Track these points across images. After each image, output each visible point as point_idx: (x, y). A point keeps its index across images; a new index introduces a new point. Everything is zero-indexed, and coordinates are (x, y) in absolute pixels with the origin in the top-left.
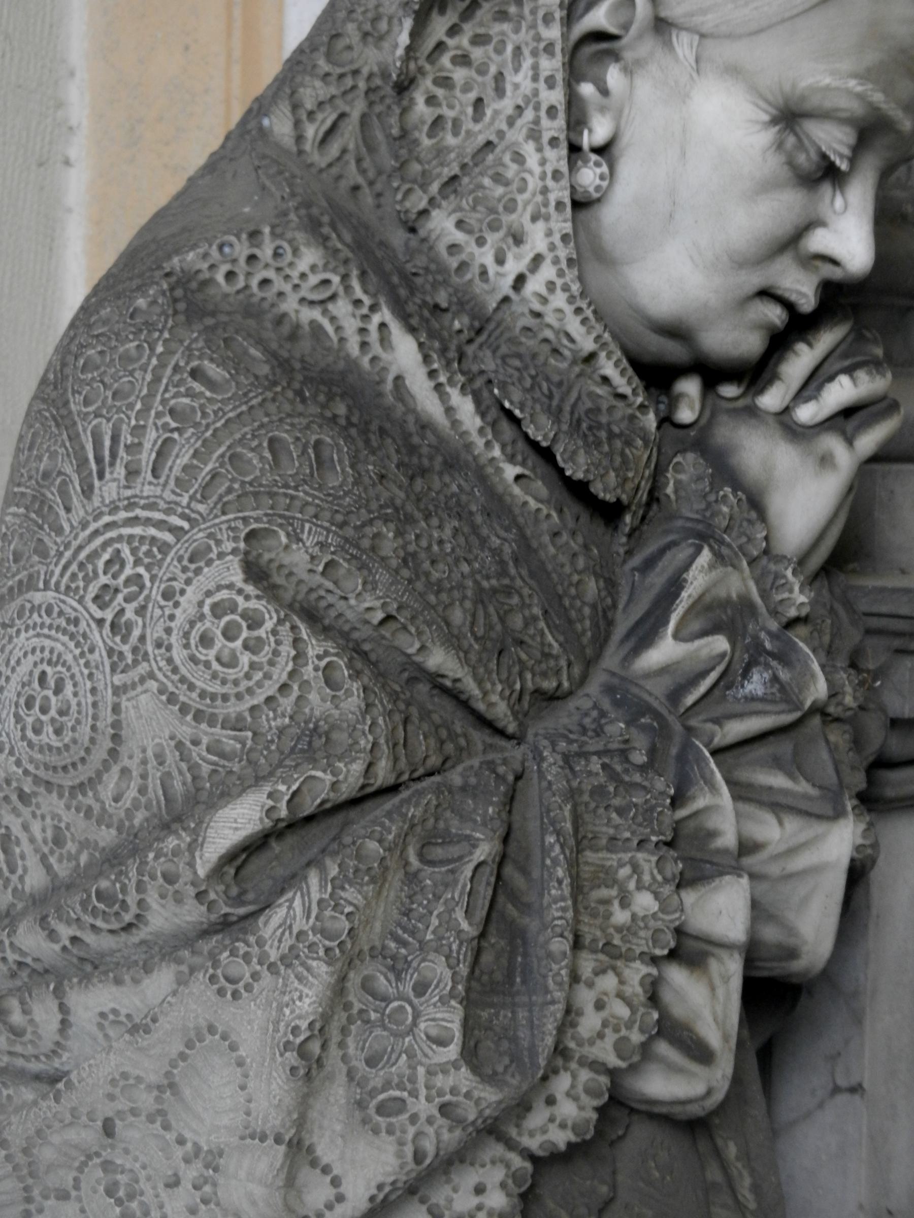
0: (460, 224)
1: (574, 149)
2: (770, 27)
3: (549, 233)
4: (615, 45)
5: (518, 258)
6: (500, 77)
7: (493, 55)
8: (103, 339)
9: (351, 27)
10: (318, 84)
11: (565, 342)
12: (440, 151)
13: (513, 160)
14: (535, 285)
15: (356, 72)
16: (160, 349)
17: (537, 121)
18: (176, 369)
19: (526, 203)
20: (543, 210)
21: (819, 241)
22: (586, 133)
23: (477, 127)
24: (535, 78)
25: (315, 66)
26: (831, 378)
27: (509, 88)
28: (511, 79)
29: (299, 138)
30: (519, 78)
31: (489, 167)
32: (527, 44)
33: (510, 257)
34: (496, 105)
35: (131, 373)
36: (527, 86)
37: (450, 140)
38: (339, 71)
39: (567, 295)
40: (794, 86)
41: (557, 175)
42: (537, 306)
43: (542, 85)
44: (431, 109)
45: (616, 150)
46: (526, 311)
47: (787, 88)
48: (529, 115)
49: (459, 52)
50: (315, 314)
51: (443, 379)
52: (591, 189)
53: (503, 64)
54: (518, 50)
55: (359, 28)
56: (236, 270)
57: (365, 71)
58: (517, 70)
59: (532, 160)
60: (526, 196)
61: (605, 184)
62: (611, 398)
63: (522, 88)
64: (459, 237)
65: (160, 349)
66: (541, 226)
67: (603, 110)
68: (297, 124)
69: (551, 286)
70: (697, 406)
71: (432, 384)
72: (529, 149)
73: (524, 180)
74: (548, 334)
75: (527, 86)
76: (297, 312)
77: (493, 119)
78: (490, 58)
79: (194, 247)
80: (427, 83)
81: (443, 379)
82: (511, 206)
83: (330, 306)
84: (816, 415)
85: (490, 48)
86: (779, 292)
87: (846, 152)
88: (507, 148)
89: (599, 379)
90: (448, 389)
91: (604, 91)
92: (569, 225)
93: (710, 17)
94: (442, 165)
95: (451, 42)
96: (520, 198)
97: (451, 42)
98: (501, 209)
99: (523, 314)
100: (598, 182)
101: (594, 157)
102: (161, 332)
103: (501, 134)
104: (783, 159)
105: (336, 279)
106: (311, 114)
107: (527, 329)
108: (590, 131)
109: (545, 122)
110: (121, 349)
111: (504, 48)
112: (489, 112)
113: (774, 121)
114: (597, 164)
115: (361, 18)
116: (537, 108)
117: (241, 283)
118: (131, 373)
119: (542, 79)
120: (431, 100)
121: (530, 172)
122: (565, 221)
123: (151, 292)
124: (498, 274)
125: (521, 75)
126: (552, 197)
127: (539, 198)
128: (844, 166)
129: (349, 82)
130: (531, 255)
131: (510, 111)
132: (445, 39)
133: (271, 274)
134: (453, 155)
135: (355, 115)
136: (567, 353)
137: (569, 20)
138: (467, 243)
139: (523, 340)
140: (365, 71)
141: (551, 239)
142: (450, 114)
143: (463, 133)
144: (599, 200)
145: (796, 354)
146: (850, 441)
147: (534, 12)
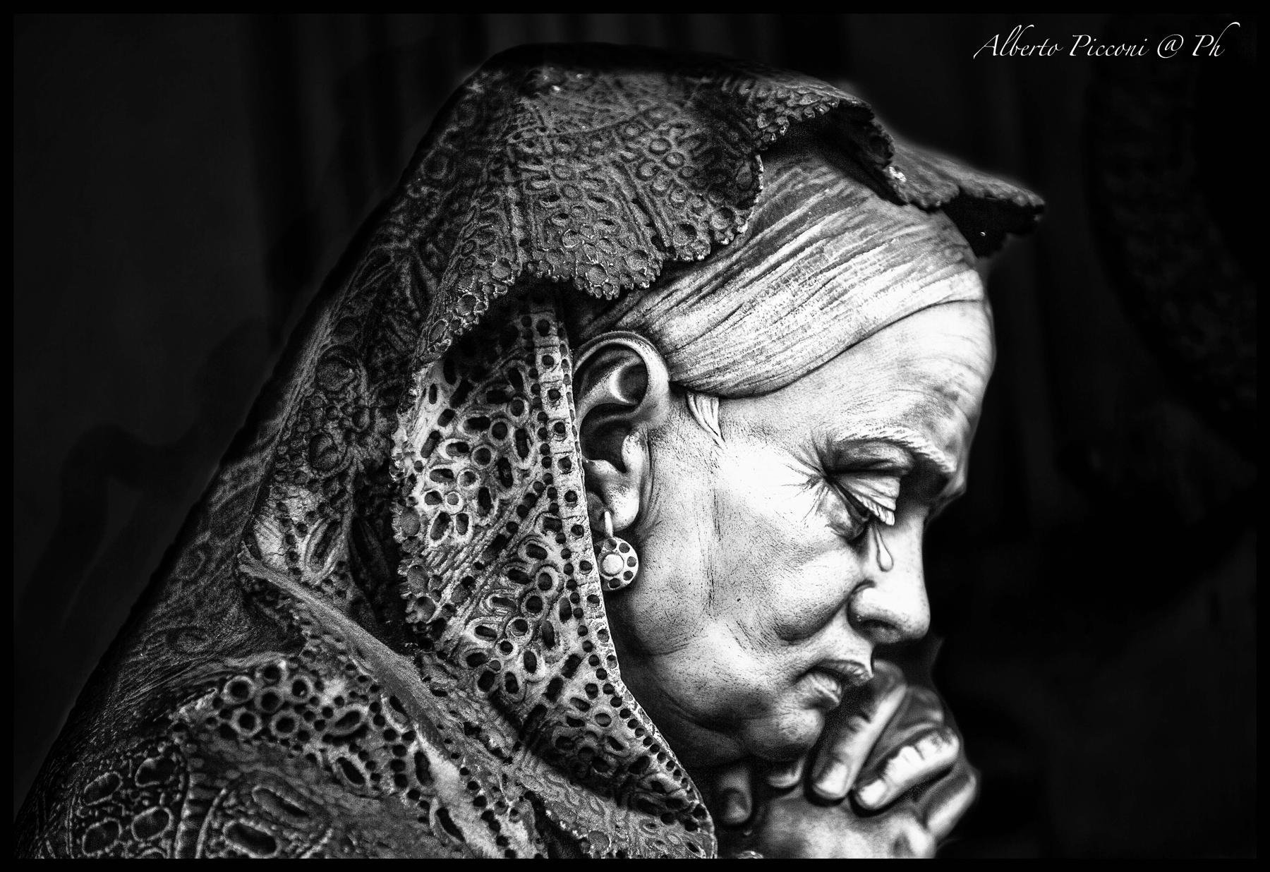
0: (481, 631)
1: (599, 535)
2: (795, 381)
3: (583, 632)
4: (628, 416)
5: (550, 661)
6: (503, 464)
7: (492, 440)
8: (109, 810)
9: (331, 425)
10: (304, 493)
11: (610, 749)
12: (449, 551)
13: (531, 554)
14: (573, 690)
15: (342, 476)
16: (186, 813)
17: (554, 509)
18: (211, 832)
19: (552, 601)
20: (573, 606)
21: (868, 603)
22: (607, 514)
23: (488, 520)
24: (547, 463)
25: (298, 474)
26: (894, 753)
27: (516, 474)
28: (518, 464)
29: (292, 556)
30: (527, 464)
31: (503, 564)
32: (533, 426)
33: (541, 661)
34: (504, 496)
35: (156, 843)
36: (537, 472)
37: (460, 540)
38: (324, 476)
39: (611, 696)
40: (829, 442)
41: (585, 566)
42: (576, 713)
43: (556, 469)
44: (433, 507)
45: (639, 532)
46: (563, 719)
47: (822, 444)
48: (544, 503)
49: (455, 441)
50: (344, 750)
51: (491, 806)
52: (621, 577)
53: (505, 451)
54: (522, 436)
55: (341, 426)
56: (252, 713)
57: (352, 471)
58: (524, 454)
59: (554, 554)
60: (551, 593)
61: (634, 570)
62: (663, 805)
63: (533, 475)
64: (482, 644)
65: (186, 813)
66: (573, 623)
67: (623, 487)
68: (289, 540)
69: (591, 690)
70: (749, 801)
71: (480, 813)
72: (549, 540)
73: (547, 576)
74: (591, 742)
75: (537, 472)
76: (323, 751)
77: (501, 511)
78: (490, 444)
79: (200, 693)
80: (424, 479)
81: (491, 806)
82: (535, 606)
83: (358, 741)
84: (883, 796)
85: (489, 432)
86: (833, 666)
87: (892, 505)
88: (522, 541)
89: (649, 786)
90: (497, 817)
91: (622, 468)
92: (605, 618)
93: (728, 376)
94: (452, 567)
95: (446, 431)
96: (545, 596)
97: (446, 431)
98: (524, 609)
99: (559, 723)
100: (627, 568)
101: (619, 541)
102: (184, 793)
103: (512, 527)
104: (825, 520)
105: (365, 710)
106: (302, 529)
107: (562, 739)
108: (612, 513)
109: (564, 511)
110: (137, 818)
111: (506, 432)
112: (496, 504)
113: (812, 482)
114: (624, 549)
115: (341, 415)
116: (553, 494)
117: (258, 728)
118: (156, 843)
119: (555, 463)
120: (434, 498)
121: (554, 566)
122: (600, 617)
123: (161, 750)
124: (528, 681)
125: (529, 460)
126: (583, 592)
127: (568, 594)
128: (889, 519)
129: (336, 486)
130: (566, 657)
131: (520, 501)
132: (437, 427)
133: (291, 713)
134: (462, 556)
135: (347, 522)
136: (612, 760)
137: (577, 397)
138: (489, 651)
139: (562, 751)
140: (352, 471)
141: (586, 638)
142: (454, 510)
143: (470, 530)
144: (629, 588)
145: (853, 730)
146: (923, 821)
147: (536, 390)
